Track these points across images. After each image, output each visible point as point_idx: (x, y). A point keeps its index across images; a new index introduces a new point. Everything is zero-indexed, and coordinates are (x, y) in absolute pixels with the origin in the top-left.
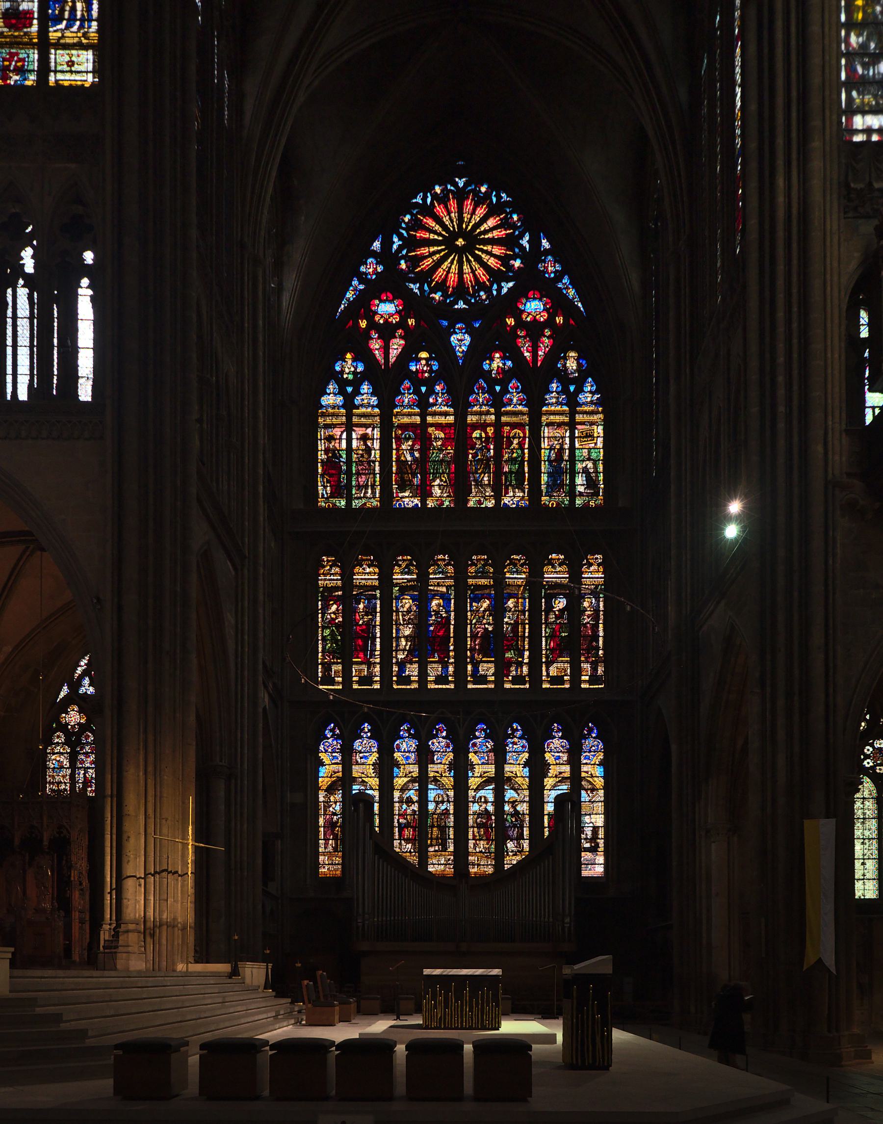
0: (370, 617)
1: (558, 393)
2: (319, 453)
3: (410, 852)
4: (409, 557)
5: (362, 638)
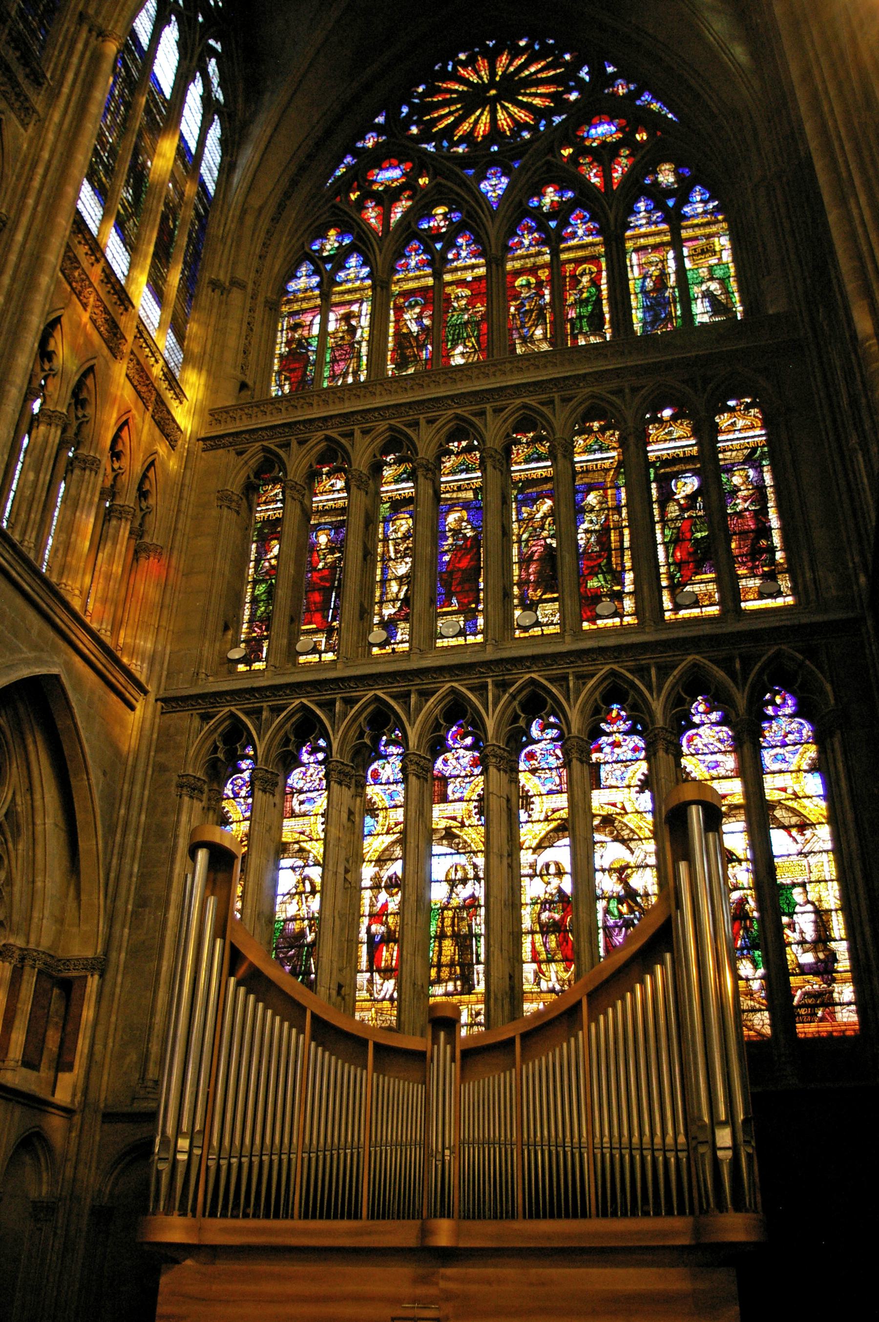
2: (278, 347)
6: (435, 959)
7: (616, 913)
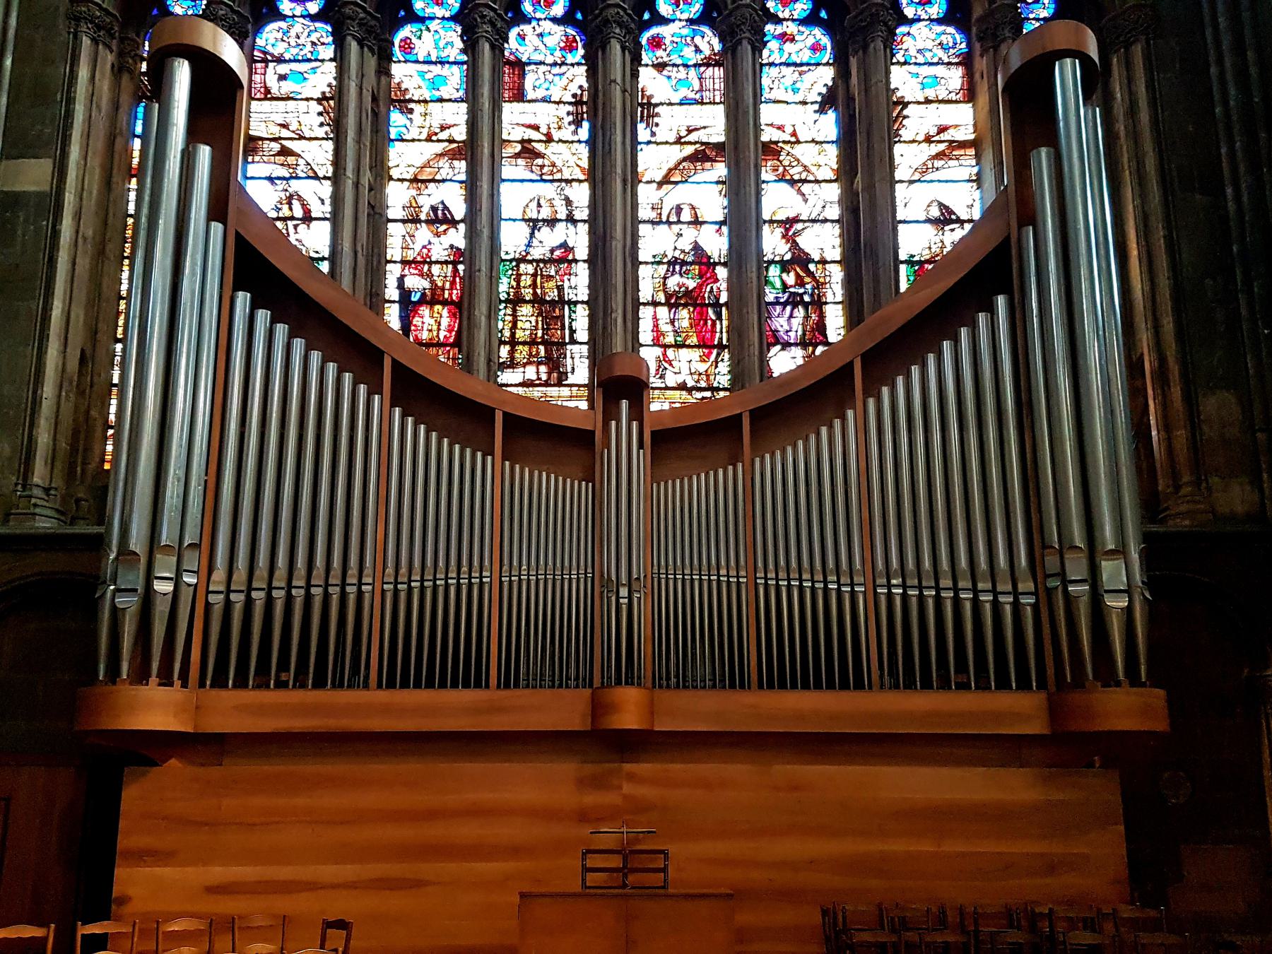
6: (507, 333)
7: (778, 284)
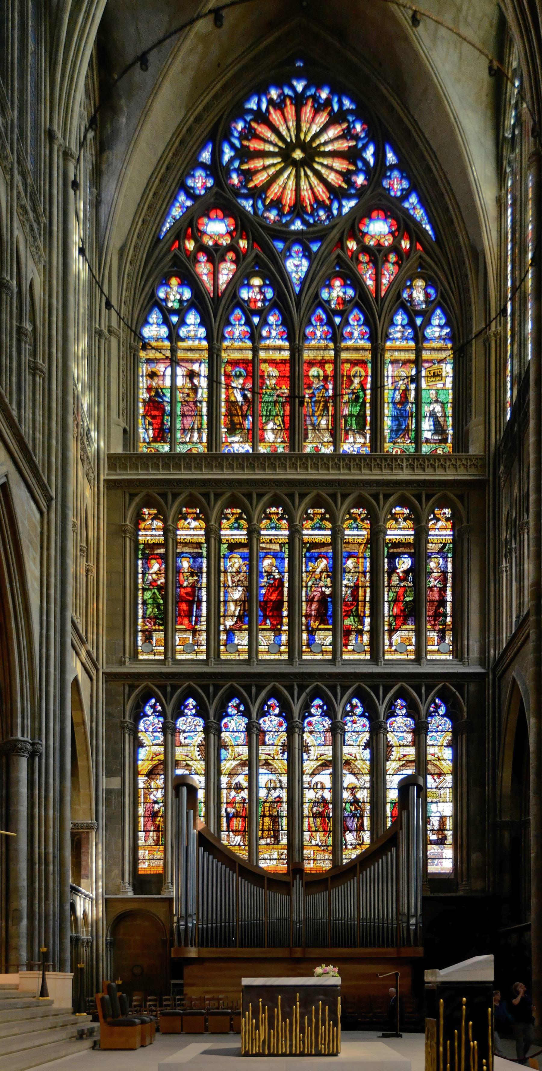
0: (196, 578)
1: (403, 326)
2: (141, 391)
3: (239, 845)
4: (239, 511)
5: (188, 602)
